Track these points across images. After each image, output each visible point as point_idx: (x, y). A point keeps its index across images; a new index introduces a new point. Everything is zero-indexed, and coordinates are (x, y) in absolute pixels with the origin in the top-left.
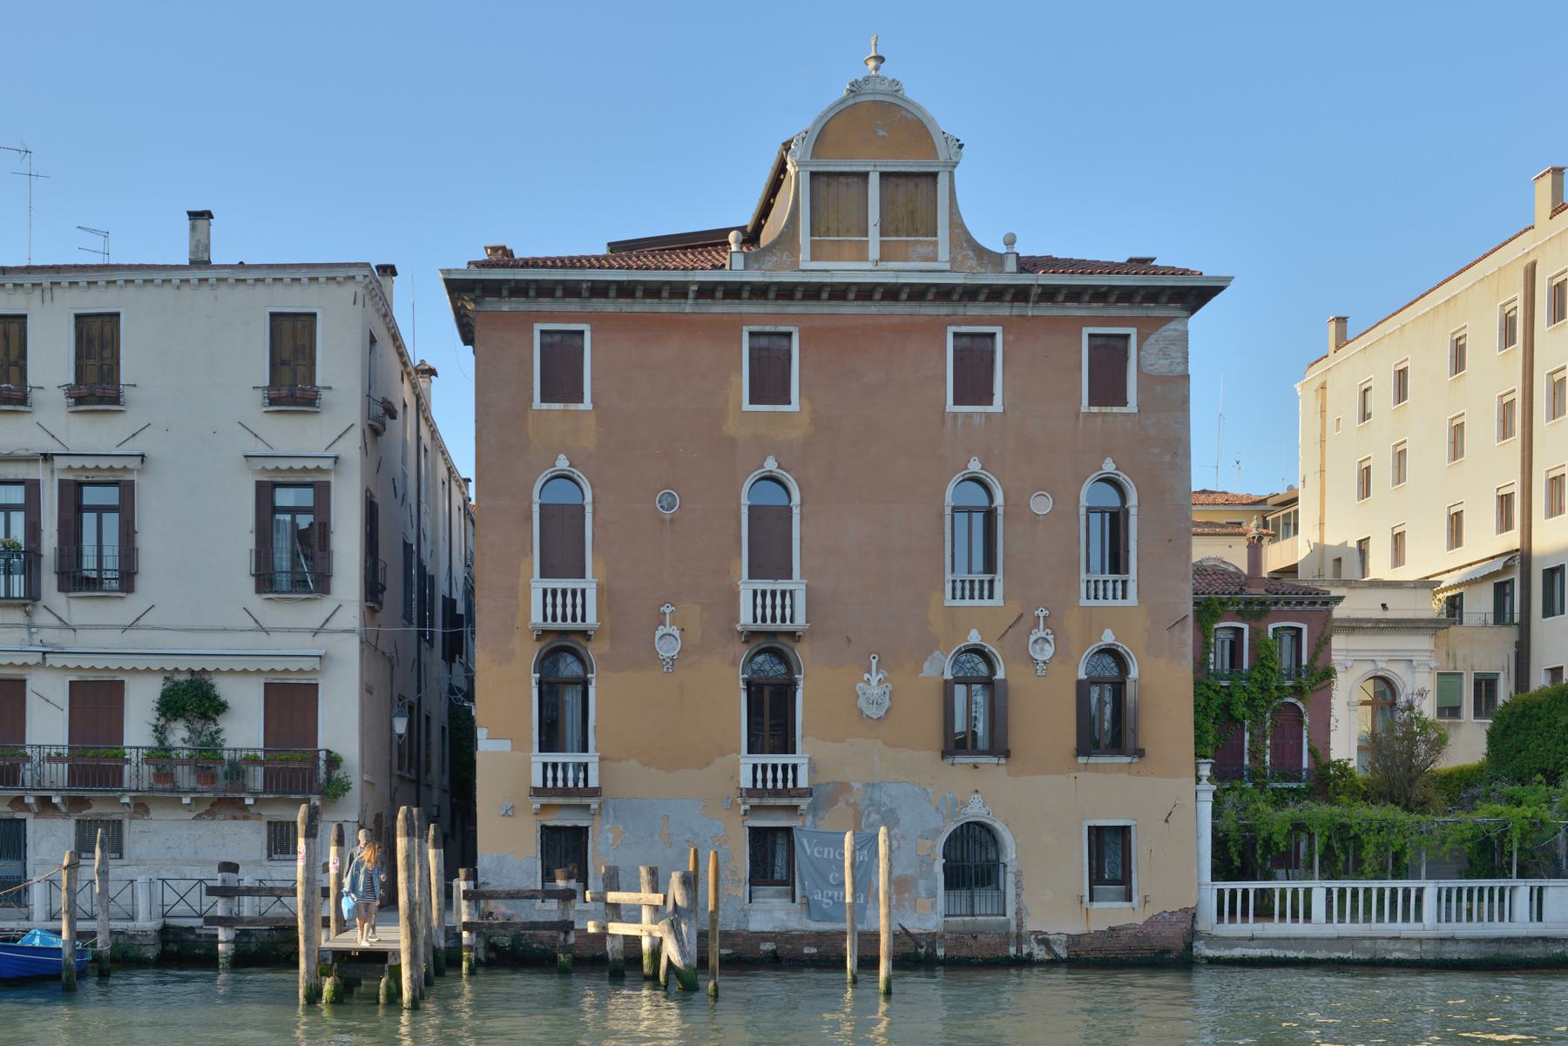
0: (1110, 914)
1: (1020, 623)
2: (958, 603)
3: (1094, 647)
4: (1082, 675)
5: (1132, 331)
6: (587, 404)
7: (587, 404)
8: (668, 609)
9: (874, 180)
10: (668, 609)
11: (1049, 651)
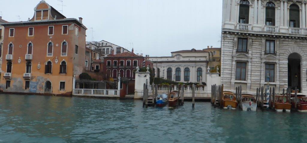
0: (62, 92)
1: (54, 59)
2: (49, 56)
3: (62, 61)
4: (61, 64)
5: (68, 25)
6: (14, 36)
7: (14, 36)
8: (20, 57)
9: (42, 11)
10: (20, 57)
11: (57, 61)
